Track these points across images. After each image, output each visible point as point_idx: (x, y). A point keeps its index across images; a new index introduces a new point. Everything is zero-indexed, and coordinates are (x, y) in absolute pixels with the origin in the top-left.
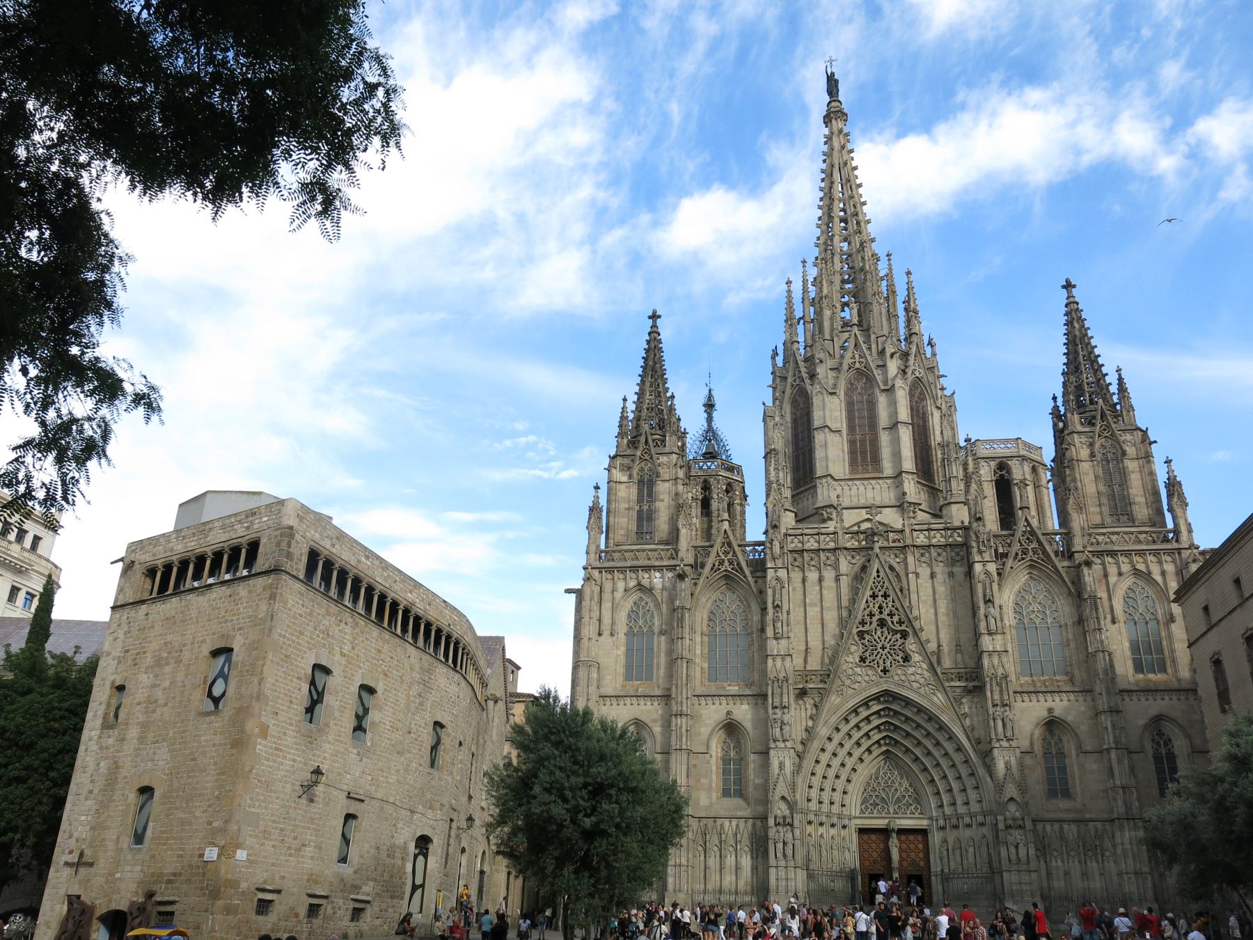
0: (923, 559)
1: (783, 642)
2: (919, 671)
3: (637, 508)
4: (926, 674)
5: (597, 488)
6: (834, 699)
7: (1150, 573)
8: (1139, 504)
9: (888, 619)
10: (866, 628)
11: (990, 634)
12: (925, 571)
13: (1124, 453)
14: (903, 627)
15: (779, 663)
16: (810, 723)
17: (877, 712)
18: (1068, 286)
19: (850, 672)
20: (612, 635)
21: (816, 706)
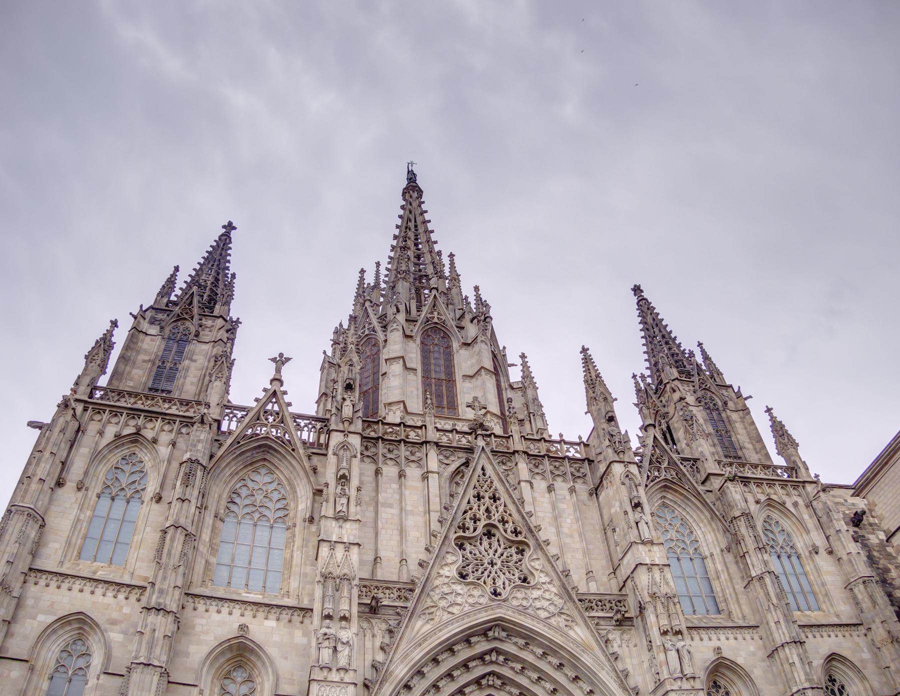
0: (536, 471)
1: (348, 525)
2: (547, 595)
3: (158, 363)
4: (559, 602)
5: (115, 324)
6: (420, 626)
7: (783, 504)
8: (748, 449)
9: (500, 526)
10: (467, 534)
11: (643, 543)
12: (541, 485)
13: (726, 403)
14: (520, 538)
15: (340, 551)
16: (380, 657)
17: (481, 657)
18: (637, 290)
19: (446, 589)
20: (79, 489)
21: (390, 632)
